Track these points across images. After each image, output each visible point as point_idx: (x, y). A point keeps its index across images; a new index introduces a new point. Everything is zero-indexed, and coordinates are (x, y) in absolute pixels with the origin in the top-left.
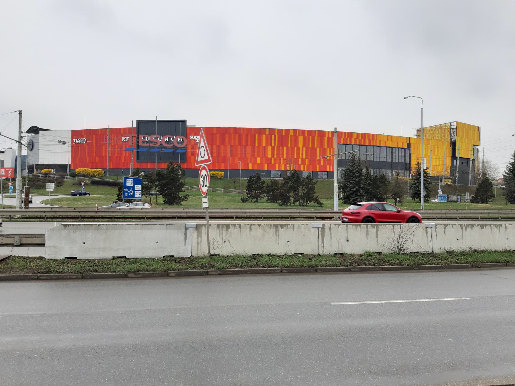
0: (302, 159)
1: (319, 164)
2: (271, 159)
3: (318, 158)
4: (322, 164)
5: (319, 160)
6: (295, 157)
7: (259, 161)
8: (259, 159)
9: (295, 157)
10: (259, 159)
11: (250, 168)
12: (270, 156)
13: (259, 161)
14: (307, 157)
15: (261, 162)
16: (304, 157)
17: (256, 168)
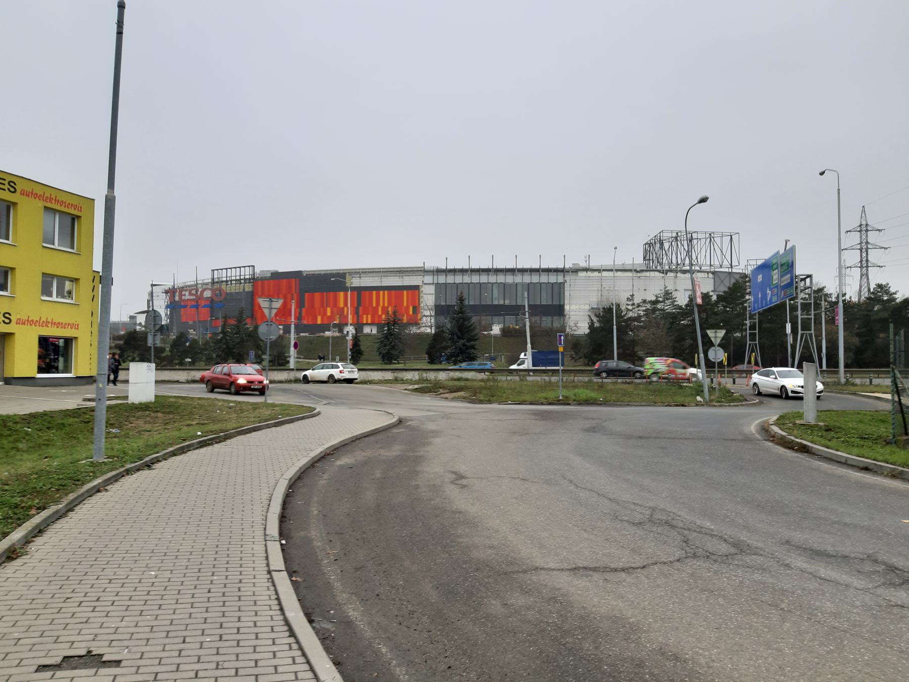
0: (383, 308)
1: (408, 314)
2: (343, 309)
3: (405, 304)
4: (411, 313)
5: (407, 308)
6: (374, 305)
7: (329, 314)
8: (329, 310)
9: (374, 305)
10: (329, 310)
11: (319, 322)
12: (342, 305)
13: (329, 314)
14: (389, 304)
15: (332, 312)
16: (386, 305)
17: (325, 322)
